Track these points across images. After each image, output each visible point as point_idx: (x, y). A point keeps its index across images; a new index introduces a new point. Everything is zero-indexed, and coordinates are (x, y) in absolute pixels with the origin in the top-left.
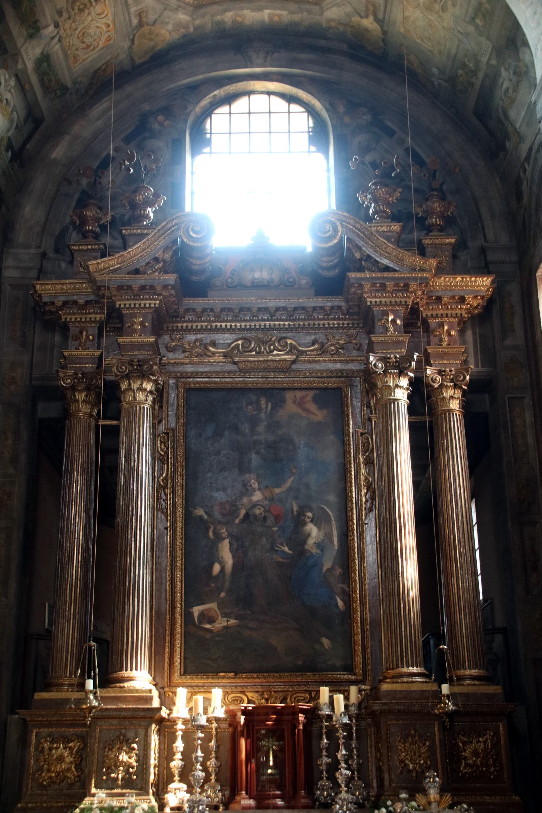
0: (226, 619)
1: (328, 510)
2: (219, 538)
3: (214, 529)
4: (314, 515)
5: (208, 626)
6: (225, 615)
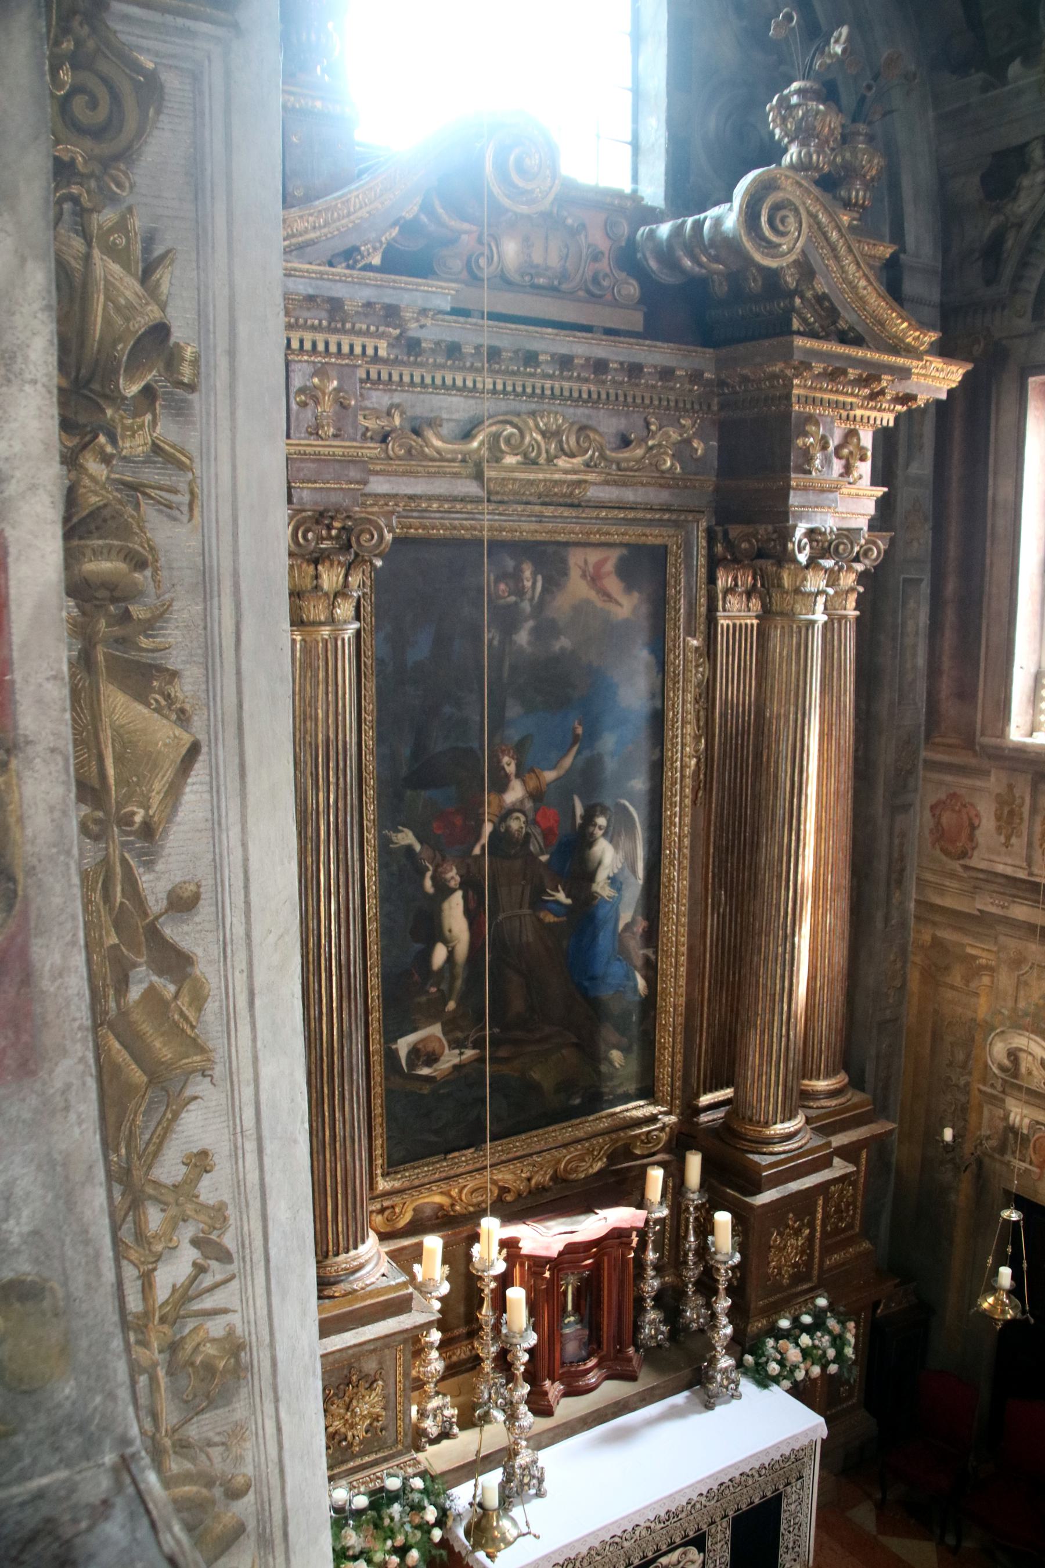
0: (457, 1051)
1: (632, 809)
2: (444, 891)
3: (435, 871)
4: (609, 821)
5: (425, 1071)
6: (457, 1044)
